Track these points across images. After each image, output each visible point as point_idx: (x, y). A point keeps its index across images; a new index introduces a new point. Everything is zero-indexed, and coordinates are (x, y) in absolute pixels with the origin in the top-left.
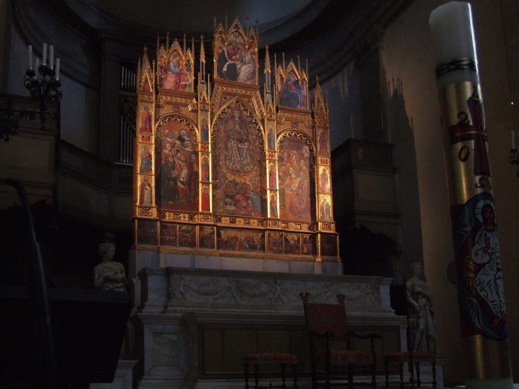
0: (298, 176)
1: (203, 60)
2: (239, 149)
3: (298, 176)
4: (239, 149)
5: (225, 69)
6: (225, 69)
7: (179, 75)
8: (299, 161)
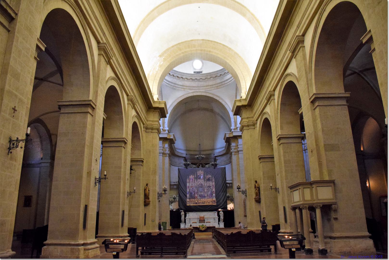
0: (210, 191)
1: (196, 176)
2: (201, 189)
3: (210, 191)
4: (201, 189)
5: (199, 177)
6: (199, 177)
7: (193, 179)
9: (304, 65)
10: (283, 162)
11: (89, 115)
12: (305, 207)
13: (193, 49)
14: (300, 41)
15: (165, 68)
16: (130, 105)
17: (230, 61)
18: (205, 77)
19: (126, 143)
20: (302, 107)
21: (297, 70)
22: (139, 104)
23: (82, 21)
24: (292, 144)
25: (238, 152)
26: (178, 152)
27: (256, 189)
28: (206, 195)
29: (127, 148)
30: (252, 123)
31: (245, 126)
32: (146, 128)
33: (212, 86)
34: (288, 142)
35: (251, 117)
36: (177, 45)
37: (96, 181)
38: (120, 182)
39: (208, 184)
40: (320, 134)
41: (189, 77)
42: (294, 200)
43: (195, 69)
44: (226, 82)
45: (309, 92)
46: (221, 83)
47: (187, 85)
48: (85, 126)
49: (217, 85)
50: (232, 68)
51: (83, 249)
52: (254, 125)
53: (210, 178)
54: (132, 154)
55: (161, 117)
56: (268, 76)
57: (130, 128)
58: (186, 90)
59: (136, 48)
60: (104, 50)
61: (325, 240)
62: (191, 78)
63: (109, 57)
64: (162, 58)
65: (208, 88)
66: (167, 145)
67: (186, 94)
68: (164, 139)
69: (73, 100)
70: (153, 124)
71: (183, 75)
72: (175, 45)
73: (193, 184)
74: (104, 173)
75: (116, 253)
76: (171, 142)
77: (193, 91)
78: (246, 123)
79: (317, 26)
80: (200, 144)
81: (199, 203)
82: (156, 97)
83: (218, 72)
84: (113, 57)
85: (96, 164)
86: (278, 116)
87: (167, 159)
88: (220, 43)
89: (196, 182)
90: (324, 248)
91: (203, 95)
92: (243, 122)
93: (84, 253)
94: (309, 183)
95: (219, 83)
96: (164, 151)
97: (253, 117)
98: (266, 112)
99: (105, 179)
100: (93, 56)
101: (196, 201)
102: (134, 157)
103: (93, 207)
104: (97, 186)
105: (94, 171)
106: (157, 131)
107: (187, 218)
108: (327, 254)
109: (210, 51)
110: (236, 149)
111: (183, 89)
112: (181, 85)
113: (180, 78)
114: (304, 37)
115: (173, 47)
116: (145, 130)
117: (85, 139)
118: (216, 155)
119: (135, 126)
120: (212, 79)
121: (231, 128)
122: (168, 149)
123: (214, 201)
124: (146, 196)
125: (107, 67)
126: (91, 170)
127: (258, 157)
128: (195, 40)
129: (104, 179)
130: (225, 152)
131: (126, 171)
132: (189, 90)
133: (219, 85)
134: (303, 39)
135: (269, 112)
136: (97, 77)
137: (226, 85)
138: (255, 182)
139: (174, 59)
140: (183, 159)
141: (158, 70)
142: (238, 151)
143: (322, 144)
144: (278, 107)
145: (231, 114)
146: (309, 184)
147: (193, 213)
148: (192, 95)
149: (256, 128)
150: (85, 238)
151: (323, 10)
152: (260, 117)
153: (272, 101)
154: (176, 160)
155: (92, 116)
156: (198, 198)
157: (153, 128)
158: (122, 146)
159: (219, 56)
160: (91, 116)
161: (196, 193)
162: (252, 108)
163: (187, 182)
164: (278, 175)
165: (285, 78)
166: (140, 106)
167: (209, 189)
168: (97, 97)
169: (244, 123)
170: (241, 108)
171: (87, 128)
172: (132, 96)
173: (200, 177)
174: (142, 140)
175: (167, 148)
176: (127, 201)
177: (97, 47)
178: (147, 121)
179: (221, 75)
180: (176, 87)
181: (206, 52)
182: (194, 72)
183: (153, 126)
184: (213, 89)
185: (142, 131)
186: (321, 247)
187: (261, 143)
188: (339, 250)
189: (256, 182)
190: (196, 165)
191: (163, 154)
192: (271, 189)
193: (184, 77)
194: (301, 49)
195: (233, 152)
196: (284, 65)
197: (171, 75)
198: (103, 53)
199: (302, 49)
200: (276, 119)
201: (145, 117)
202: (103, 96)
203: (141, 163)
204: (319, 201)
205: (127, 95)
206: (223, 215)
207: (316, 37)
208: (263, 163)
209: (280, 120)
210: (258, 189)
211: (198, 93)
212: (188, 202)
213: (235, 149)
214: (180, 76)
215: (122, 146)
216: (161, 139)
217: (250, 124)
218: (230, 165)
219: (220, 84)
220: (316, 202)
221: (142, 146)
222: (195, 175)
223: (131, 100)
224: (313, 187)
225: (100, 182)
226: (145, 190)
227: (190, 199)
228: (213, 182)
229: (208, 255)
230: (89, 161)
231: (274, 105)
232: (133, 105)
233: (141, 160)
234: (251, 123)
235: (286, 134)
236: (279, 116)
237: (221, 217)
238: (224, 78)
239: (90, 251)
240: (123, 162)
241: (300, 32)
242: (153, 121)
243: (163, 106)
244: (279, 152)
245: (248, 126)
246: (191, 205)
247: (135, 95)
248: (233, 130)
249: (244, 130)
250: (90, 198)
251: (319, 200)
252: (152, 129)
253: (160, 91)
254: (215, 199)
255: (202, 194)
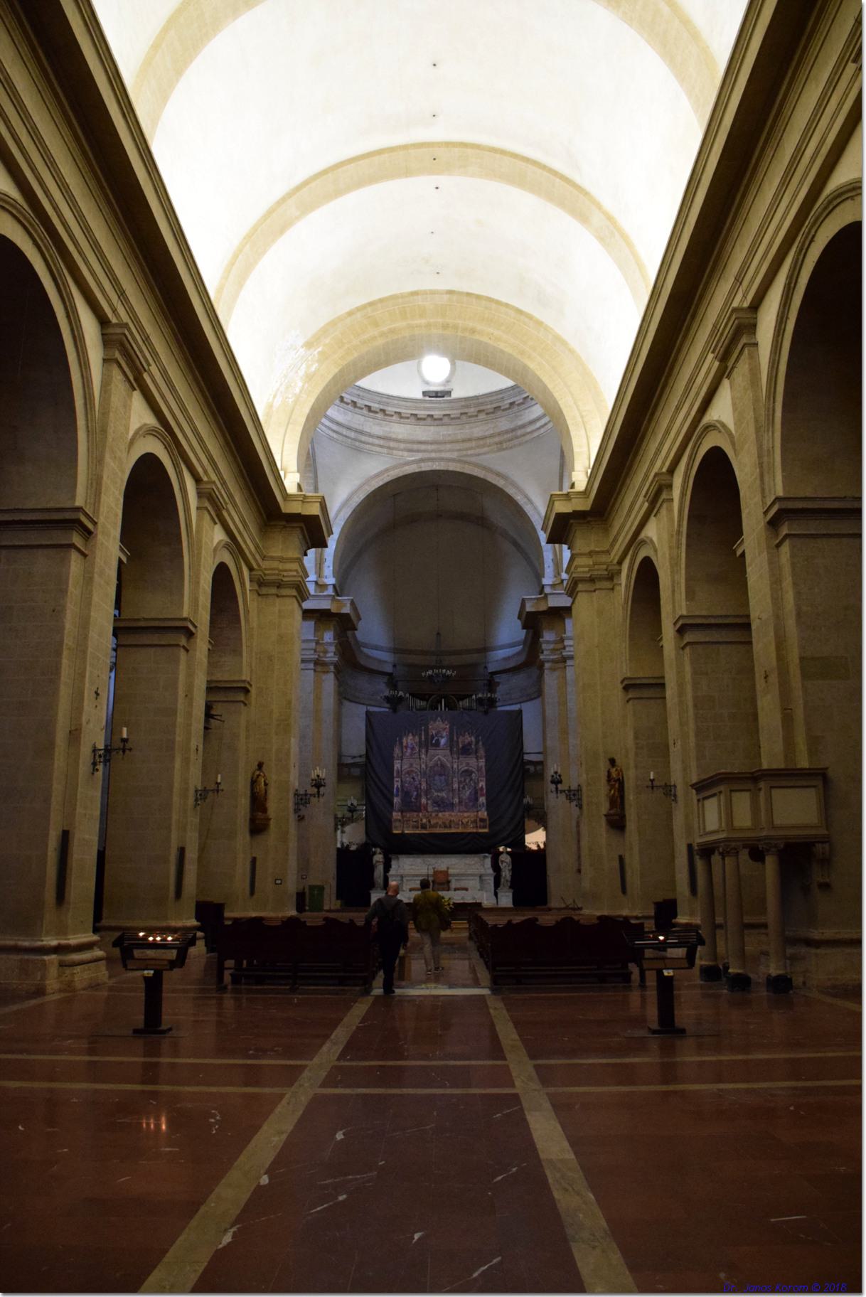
5: (434, 742)
6: (434, 742)
7: (413, 749)
8: (470, 782)
9: (754, 405)
10: (690, 704)
11: (74, 556)
12: (732, 849)
13: (418, 322)
14: (744, 325)
15: (324, 384)
16: (206, 512)
17: (537, 365)
18: (459, 411)
19: (190, 635)
20: (743, 535)
21: (734, 417)
22: (235, 505)
23: (53, 262)
24: (722, 647)
25: (565, 662)
26: (368, 657)
27: (612, 787)
28: (456, 800)
29: (195, 650)
30: (606, 570)
31: (583, 580)
32: (258, 583)
33: (481, 442)
34: (707, 639)
35: (603, 552)
36: (364, 307)
37: (97, 757)
38: (172, 758)
39: (464, 765)
40: (791, 623)
41: (407, 408)
42: (704, 829)
43: (427, 383)
44: (529, 430)
45: (763, 490)
46: (513, 430)
47: (400, 437)
48: (63, 591)
49: (497, 439)
50: (545, 387)
51: (56, 964)
52: (612, 576)
53: (470, 744)
54: (212, 665)
55: (310, 544)
56: (653, 424)
57: (207, 588)
58: (395, 452)
59: (224, 328)
60: (122, 344)
61: (790, 951)
62: (414, 412)
63: (139, 364)
64: (316, 352)
65: (471, 448)
66: (328, 636)
67: (394, 468)
68: (319, 617)
69: (24, 507)
70: (281, 567)
71: (387, 404)
72: (358, 309)
73: (414, 765)
74: (121, 732)
75: (152, 972)
76: (344, 624)
77: (419, 456)
78: (587, 569)
79: (792, 285)
80: (438, 634)
81: (435, 826)
82: (291, 481)
83: (501, 396)
84: (149, 365)
85: (96, 706)
86: (679, 556)
87: (329, 682)
88: (507, 305)
89: (423, 756)
90: (781, 972)
91: (451, 469)
92: (576, 567)
93: (59, 976)
94: (748, 775)
95: (507, 432)
96: (321, 654)
97: (608, 552)
98: (648, 537)
99: (124, 751)
100: (86, 368)
101: (424, 821)
102: (219, 676)
103: (87, 837)
104: (100, 774)
105: (91, 725)
106: (294, 590)
107: (392, 875)
108: (791, 992)
109: (473, 331)
110: (557, 650)
111: (385, 450)
112: (379, 437)
113: (376, 412)
114: (756, 314)
115: (350, 314)
116: (256, 587)
117: (60, 630)
118: (491, 668)
119: (222, 574)
120: (482, 416)
121: (544, 583)
122: (332, 649)
123: (482, 820)
124: (258, 802)
125: (130, 397)
126: (81, 725)
127: (622, 682)
128: (425, 293)
129: (121, 752)
130: (522, 659)
131: (190, 725)
132: (406, 454)
133: (506, 436)
134: (752, 321)
135: (655, 539)
136: (99, 434)
137: (528, 437)
138: (608, 762)
139: (356, 355)
140: (385, 679)
141: (301, 392)
142: (564, 660)
143: (794, 655)
144: (680, 526)
145: (543, 537)
146: (747, 778)
147: (411, 859)
148: (417, 470)
149: (617, 588)
150: (62, 931)
151: (807, 237)
152: (631, 552)
153: (665, 505)
154: (363, 683)
155: (85, 555)
156: (430, 809)
157: (282, 580)
158: (178, 645)
159: (502, 346)
160: (82, 557)
161: (422, 794)
162: (606, 520)
163: (395, 756)
164: (674, 744)
165: (701, 437)
166: (240, 511)
167: (465, 780)
168: (100, 498)
169: (579, 570)
170: (572, 521)
171: (69, 594)
172: (214, 482)
173: (438, 740)
174: (247, 620)
175: (330, 644)
176: (194, 820)
177: (100, 337)
178: (264, 558)
179: (512, 404)
180: (361, 442)
181: (460, 334)
182: (425, 393)
183: (283, 576)
184: (486, 449)
185: (244, 594)
186: (774, 970)
187: (632, 638)
188: (829, 979)
189: (612, 762)
190: (427, 701)
191: (317, 663)
192: (653, 788)
193: (390, 409)
194: (746, 351)
195: (548, 661)
196: (697, 394)
197: (348, 404)
198: (117, 355)
199: (749, 350)
200: (674, 564)
201: (257, 547)
202: (117, 493)
203: (241, 697)
204: (772, 833)
205: (198, 480)
206: (510, 867)
207: (787, 318)
208: (636, 701)
209: (687, 566)
210: (617, 785)
211: (437, 463)
212: (396, 820)
213: (554, 651)
214: (375, 406)
215: (178, 645)
216: (308, 614)
217: (599, 573)
218: (537, 702)
219: (509, 435)
220: (764, 833)
221: (244, 641)
222: (420, 735)
223: (210, 494)
224: (760, 789)
225: (107, 761)
226: (254, 782)
227: (402, 812)
228: (481, 759)
229: (435, 988)
230: (74, 695)
231: (671, 519)
232: (216, 511)
233: (243, 685)
234: (601, 571)
235: (704, 613)
236: (683, 555)
237: (503, 874)
238: (521, 415)
239: (79, 970)
240: (181, 694)
241: (745, 296)
242: (283, 558)
243: (314, 510)
244: (680, 672)
245: (592, 580)
246: (406, 832)
247: (222, 478)
248: (547, 590)
249: (579, 594)
250: (79, 810)
251: (774, 827)
252: (279, 585)
253: (308, 458)
254: (486, 814)
255: (443, 798)
